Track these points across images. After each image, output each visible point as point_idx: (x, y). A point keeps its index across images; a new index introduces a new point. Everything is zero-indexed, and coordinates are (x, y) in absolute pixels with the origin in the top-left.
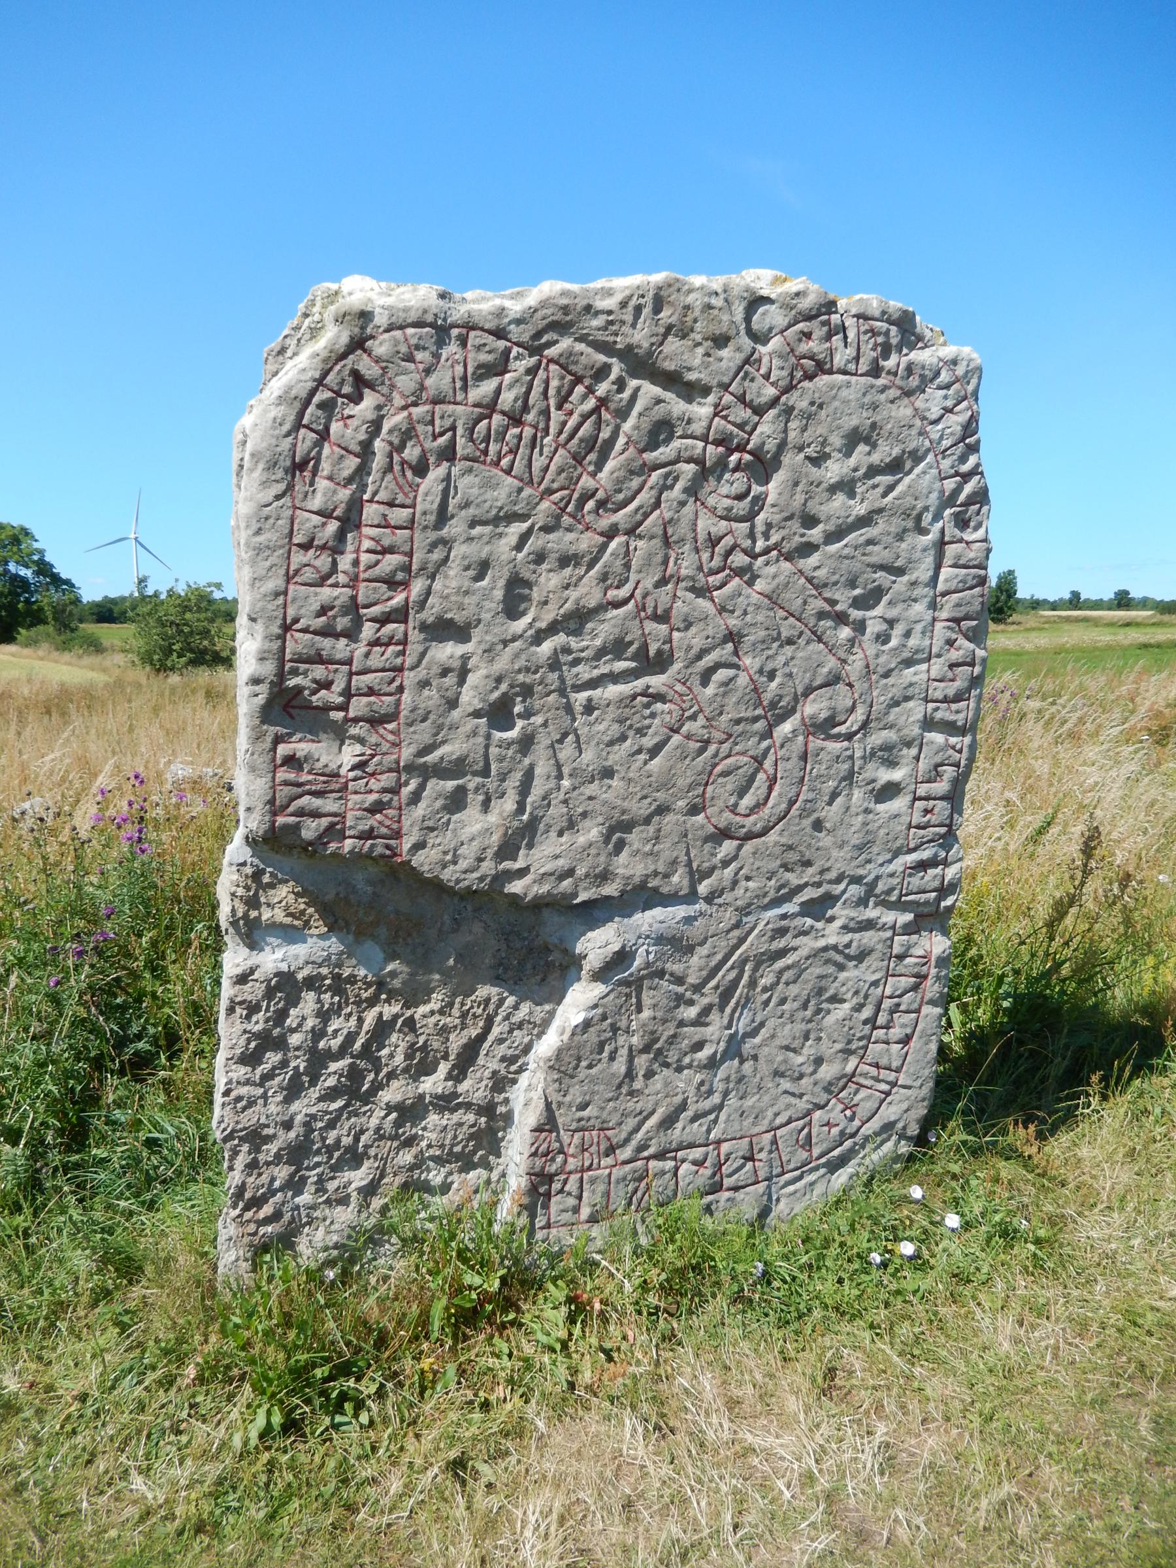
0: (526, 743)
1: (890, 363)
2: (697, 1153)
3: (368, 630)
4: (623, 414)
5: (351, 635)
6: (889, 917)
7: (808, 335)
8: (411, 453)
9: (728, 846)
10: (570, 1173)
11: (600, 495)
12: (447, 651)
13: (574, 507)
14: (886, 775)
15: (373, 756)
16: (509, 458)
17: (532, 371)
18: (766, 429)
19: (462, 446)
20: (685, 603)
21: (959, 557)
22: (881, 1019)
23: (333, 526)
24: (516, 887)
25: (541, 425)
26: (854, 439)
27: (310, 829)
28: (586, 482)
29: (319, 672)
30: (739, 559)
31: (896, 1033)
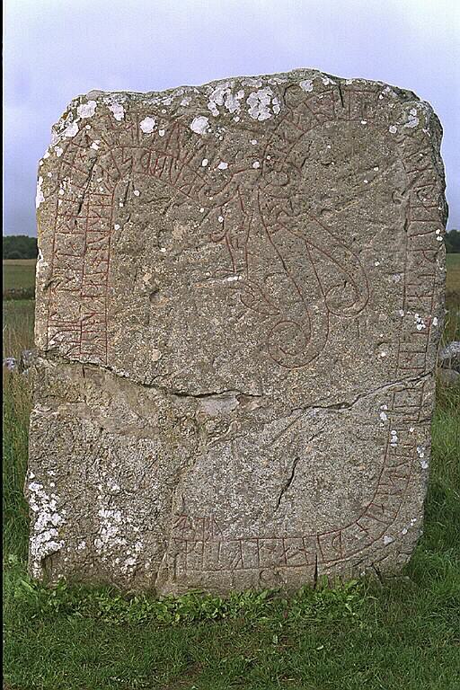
2: (269, 541)
7: (320, 103)
10: (197, 541)
11: (206, 187)
15: (93, 314)
16: (160, 171)
21: (419, 214)
23: (76, 206)
25: (176, 155)
27: (63, 349)
30: (283, 218)
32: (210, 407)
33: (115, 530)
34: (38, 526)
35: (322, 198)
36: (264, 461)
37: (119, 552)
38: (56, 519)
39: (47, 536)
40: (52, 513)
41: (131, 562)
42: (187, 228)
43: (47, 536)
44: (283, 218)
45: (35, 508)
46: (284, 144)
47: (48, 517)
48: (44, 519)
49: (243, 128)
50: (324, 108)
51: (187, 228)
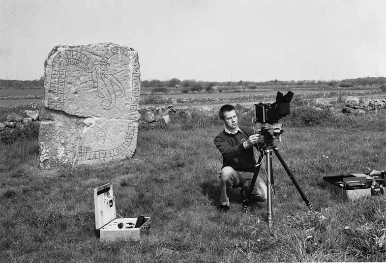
0: (79, 96)
1: (125, 53)
2: (101, 152)
3: (60, 84)
4: (91, 59)
5: (58, 84)
6: (127, 120)
8: (66, 64)
9: (105, 111)
12: (70, 86)
13: (84, 69)
14: (127, 102)
17: (80, 55)
18: (109, 61)
19: (72, 63)
20: (100, 80)
22: (128, 135)
24: (77, 114)
26: (121, 61)
28: (87, 67)
29: (54, 88)
30: (106, 75)
31: (130, 137)
32: (86, 121)
33: (63, 152)
34: (43, 153)
35: (115, 71)
36: (101, 132)
37: (63, 158)
38: (48, 151)
39: (45, 155)
40: (46, 149)
41: (67, 160)
42: (84, 78)
43: (45, 155)
44: (106, 75)
45: (42, 148)
46: (106, 59)
47: (45, 150)
48: (44, 151)
49: (97, 55)
50: (115, 51)
51: (84, 78)
